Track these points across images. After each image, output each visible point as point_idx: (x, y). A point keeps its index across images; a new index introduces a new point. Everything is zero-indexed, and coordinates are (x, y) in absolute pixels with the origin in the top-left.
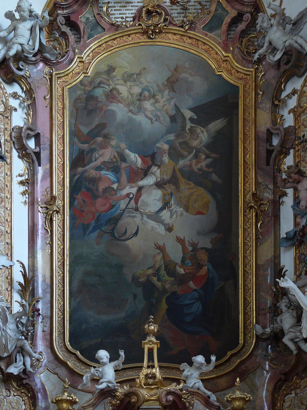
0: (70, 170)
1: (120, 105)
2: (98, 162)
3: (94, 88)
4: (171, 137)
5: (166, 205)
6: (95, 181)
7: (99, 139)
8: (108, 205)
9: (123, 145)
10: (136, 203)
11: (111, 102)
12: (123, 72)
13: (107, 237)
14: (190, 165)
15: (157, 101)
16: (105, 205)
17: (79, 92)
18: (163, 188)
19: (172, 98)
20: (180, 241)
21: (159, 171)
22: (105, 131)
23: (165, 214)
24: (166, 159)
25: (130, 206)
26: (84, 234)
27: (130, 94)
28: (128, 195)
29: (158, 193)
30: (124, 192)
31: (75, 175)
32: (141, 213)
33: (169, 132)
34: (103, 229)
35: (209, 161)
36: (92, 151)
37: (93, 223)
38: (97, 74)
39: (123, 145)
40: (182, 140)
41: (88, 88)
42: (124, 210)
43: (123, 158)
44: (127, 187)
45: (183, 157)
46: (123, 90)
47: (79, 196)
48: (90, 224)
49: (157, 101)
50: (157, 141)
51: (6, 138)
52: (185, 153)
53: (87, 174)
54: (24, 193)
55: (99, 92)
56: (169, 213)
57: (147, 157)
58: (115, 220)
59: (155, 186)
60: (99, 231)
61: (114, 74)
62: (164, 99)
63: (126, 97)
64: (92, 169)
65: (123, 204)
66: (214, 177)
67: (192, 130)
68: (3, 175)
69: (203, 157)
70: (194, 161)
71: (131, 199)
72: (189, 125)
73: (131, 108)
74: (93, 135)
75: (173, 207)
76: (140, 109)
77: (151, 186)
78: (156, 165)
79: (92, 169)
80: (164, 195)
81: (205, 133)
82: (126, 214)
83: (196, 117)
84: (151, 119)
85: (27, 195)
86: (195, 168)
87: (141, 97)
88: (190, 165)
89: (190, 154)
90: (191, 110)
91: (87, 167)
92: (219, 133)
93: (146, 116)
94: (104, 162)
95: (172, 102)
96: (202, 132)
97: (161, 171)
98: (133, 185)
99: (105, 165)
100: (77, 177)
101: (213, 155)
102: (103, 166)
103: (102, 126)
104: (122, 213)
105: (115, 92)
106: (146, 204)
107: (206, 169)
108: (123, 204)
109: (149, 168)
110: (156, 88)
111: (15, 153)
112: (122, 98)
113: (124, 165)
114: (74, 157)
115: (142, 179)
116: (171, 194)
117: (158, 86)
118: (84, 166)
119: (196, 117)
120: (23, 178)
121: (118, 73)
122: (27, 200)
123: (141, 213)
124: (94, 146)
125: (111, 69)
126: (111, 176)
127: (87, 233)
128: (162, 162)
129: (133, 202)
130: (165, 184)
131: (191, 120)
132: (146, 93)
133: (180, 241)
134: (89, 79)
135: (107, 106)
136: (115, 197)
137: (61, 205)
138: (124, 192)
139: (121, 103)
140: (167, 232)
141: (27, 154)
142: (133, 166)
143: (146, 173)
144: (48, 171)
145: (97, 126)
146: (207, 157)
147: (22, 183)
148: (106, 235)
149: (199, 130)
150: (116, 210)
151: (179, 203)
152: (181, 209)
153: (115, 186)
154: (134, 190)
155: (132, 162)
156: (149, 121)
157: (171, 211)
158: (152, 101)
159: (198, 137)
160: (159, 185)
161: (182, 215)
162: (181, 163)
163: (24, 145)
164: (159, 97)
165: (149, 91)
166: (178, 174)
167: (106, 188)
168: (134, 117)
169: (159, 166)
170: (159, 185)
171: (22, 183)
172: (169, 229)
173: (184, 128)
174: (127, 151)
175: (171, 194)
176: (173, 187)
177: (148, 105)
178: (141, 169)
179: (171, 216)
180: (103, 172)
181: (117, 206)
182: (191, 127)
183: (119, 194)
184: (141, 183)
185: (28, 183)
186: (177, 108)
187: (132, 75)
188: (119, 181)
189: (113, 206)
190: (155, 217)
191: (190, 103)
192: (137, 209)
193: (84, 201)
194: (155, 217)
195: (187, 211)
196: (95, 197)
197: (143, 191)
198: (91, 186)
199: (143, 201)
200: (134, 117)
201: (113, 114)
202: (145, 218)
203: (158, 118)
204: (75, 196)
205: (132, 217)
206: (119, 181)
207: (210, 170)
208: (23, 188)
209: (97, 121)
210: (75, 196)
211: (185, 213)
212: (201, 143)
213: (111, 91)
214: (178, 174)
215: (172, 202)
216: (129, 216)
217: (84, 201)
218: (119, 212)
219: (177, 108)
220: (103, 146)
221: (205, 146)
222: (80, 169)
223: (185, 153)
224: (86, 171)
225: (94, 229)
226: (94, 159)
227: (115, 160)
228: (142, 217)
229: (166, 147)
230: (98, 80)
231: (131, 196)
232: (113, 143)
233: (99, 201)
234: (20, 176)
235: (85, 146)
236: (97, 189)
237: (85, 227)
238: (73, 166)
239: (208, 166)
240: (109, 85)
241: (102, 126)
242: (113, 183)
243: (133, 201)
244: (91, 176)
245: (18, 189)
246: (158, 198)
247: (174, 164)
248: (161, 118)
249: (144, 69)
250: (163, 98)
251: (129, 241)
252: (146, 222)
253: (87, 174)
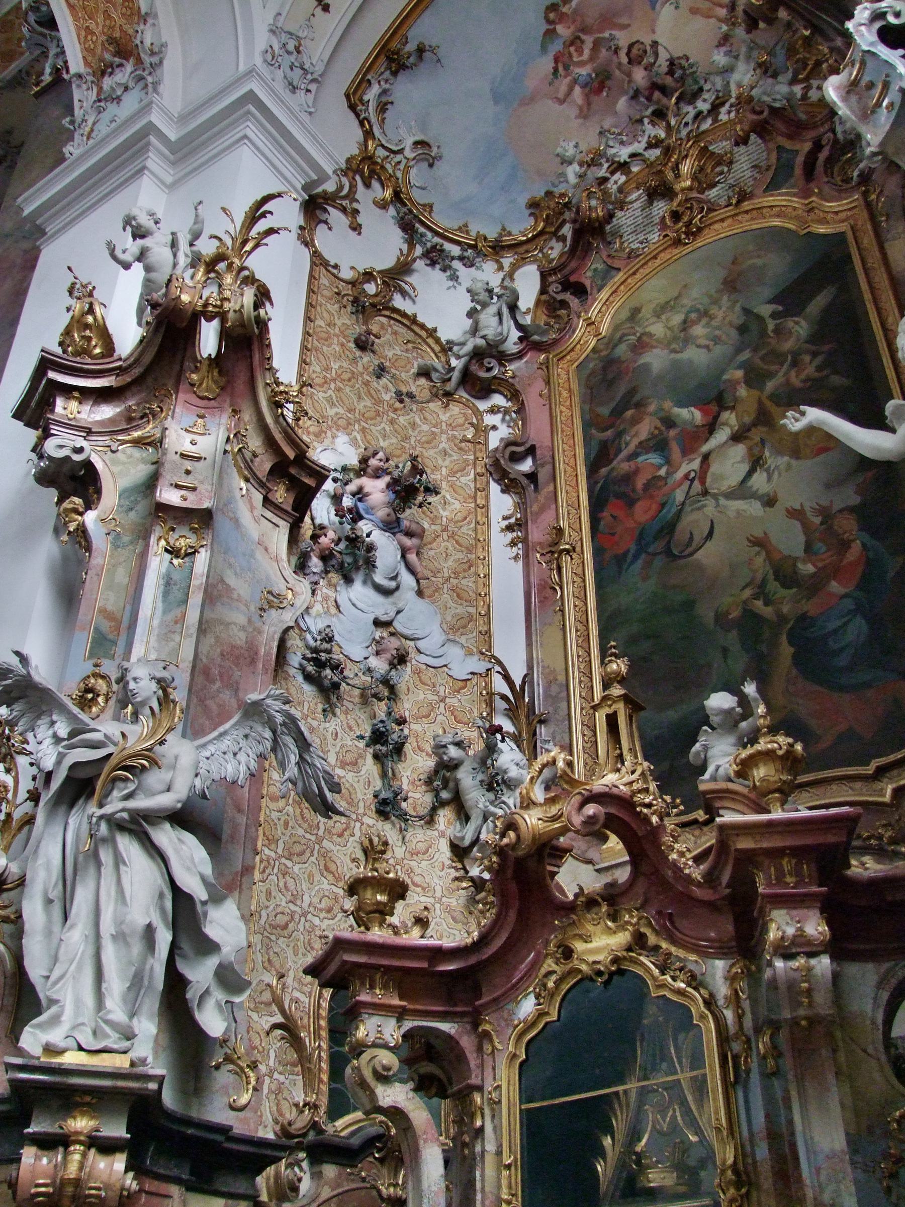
0: (589, 477)
1: (655, 351)
2: (632, 447)
3: (613, 349)
4: (746, 355)
5: (756, 463)
6: (628, 478)
7: (629, 413)
8: (654, 507)
9: (667, 404)
10: (703, 482)
11: (641, 354)
12: (653, 306)
13: (658, 562)
14: (788, 383)
15: (711, 318)
16: (649, 509)
17: (591, 365)
18: (746, 438)
19: (735, 302)
20: (795, 514)
21: (733, 415)
22: (637, 398)
23: (759, 481)
24: (742, 391)
25: (692, 492)
26: (620, 573)
27: (669, 328)
28: (686, 477)
29: (740, 450)
30: (679, 475)
31: (596, 483)
32: (715, 497)
33: (739, 350)
34: (650, 550)
35: (819, 360)
36: (619, 434)
37: (633, 548)
38: (616, 328)
39: (667, 404)
40: (764, 352)
41: (604, 353)
42: (683, 504)
43: (669, 422)
44: (684, 465)
45: (771, 375)
46: (657, 329)
47: (606, 514)
48: (628, 551)
49: (711, 318)
50: (723, 371)
51: (478, 470)
52: (773, 368)
53: (615, 474)
54: (513, 544)
55: (622, 350)
56: (765, 475)
57: (709, 403)
58: (670, 527)
59: (731, 442)
60: (643, 556)
61: (641, 315)
62: (724, 309)
63: (662, 335)
64: (622, 461)
65: (679, 496)
66: (837, 380)
67: (778, 331)
68: (473, 525)
69: (807, 358)
70: (793, 373)
71: (692, 480)
72: (771, 325)
73: (674, 346)
74: (617, 412)
75: (769, 462)
76: (687, 341)
77: (726, 442)
78: (727, 409)
79: (622, 461)
80: (750, 449)
81: (803, 323)
82: (688, 508)
83: (780, 308)
84: (707, 347)
85: (520, 545)
86: (796, 381)
87: (686, 325)
88: (788, 383)
89: (782, 365)
90: (770, 302)
91: (615, 462)
92: (827, 311)
93: (698, 346)
94: (640, 443)
95: (738, 308)
96: (797, 323)
97: (737, 416)
98: (692, 456)
99: (644, 447)
100: (599, 485)
101: (826, 348)
102: (639, 450)
103: (632, 392)
104: (680, 513)
105: (645, 338)
106: (719, 478)
107: (816, 375)
108: (679, 496)
109: (716, 417)
110: (706, 300)
111: (494, 488)
112: (658, 341)
113: (672, 433)
114: (592, 456)
115: (707, 440)
116: (763, 441)
117: (710, 297)
118: (611, 462)
119: (780, 308)
120: (513, 520)
121: (646, 312)
122: (521, 552)
123: (715, 497)
124: (621, 428)
125: (635, 312)
126: (654, 459)
127: (625, 567)
128: (736, 399)
129: (696, 483)
130: (749, 430)
131: (774, 315)
132: (693, 316)
133: (795, 514)
134: (606, 340)
135: (635, 362)
136: (665, 489)
137: (578, 538)
138: (679, 475)
139: (655, 347)
140: (767, 509)
141: (512, 480)
142: (689, 428)
143: (711, 428)
144: (552, 495)
145: (623, 397)
146: (814, 355)
147: (509, 528)
148: (659, 558)
149: (790, 323)
150: (669, 511)
151: (779, 452)
152: (786, 459)
153: (662, 472)
154: (696, 464)
155: (685, 422)
156: (704, 350)
157: (767, 470)
158: (704, 321)
159: (791, 332)
160: (736, 438)
161: (789, 467)
162: (770, 386)
163: (504, 470)
164: (714, 310)
165: (698, 310)
166: (768, 404)
167: (649, 481)
168: (679, 356)
169: (733, 408)
170: (736, 438)
171: (509, 528)
172: (770, 502)
173: (763, 333)
174: (676, 410)
175: (763, 441)
176: (764, 429)
177: (699, 330)
178: (703, 426)
179: (769, 479)
180: (640, 459)
181: (670, 501)
182: (776, 325)
183: (670, 482)
184: (705, 448)
185: (520, 525)
186: (747, 311)
187: (667, 303)
188: (668, 462)
189: (663, 505)
190: (742, 491)
191: (767, 292)
192: (705, 493)
193: (614, 517)
194: (742, 491)
195: (798, 458)
196: (631, 502)
197: (712, 458)
198: (622, 489)
199: (713, 474)
200: (679, 356)
201: (646, 367)
202: (722, 501)
203: (716, 340)
204: (600, 515)
205: (698, 509)
206: (668, 462)
207: (825, 373)
208: (510, 536)
209: (622, 389)
210: (600, 515)
211: (794, 462)
212: (798, 340)
213: (640, 338)
214: (768, 404)
215: (767, 453)
216: (693, 510)
217: (614, 517)
218: (674, 510)
219: (747, 311)
220: (635, 421)
221: (806, 342)
222: (604, 471)
223: (773, 368)
224: (613, 469)
225: (636, 557)
226: (623, 446)
227: (657, 432)
228: (717, 500)
229: (739, 374)
230: (618, 335)
231: (692, 475)
232: (652, 408)
233: (639, 507)
234: (505, 518)
235: (609, 433)
236: (634, 490)
237: (620, 560)
238: (592, 470)
239: (819, 369)
240: (634, 334)
241: (632, 392)
242: (659, 467)
243: (696, 483)
244: (622, 472)
245: (499, 540)
246: (739, 458)
247: (755, 393)
248: (724, 337)
249: (685, 286)
250: (720, 308)
251: (700, 552)
252: (725, 507)
253: (615, 474)
